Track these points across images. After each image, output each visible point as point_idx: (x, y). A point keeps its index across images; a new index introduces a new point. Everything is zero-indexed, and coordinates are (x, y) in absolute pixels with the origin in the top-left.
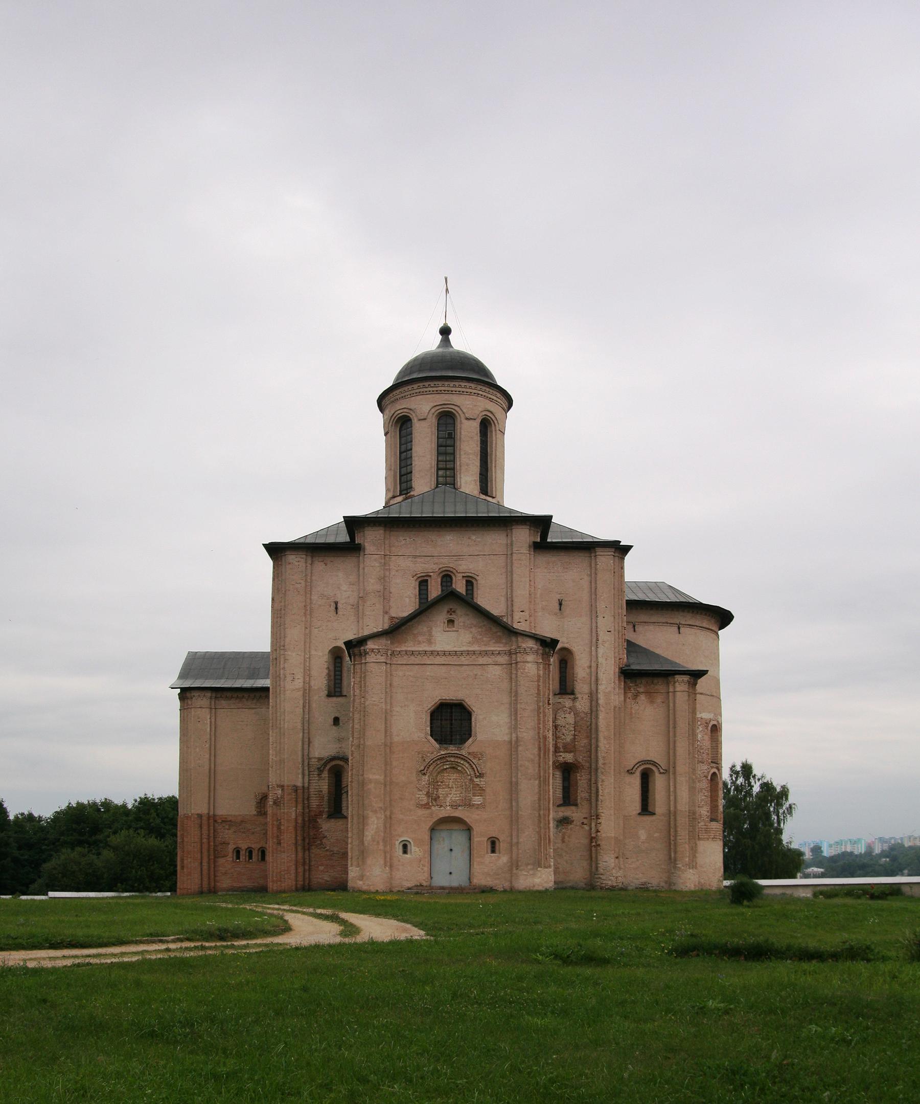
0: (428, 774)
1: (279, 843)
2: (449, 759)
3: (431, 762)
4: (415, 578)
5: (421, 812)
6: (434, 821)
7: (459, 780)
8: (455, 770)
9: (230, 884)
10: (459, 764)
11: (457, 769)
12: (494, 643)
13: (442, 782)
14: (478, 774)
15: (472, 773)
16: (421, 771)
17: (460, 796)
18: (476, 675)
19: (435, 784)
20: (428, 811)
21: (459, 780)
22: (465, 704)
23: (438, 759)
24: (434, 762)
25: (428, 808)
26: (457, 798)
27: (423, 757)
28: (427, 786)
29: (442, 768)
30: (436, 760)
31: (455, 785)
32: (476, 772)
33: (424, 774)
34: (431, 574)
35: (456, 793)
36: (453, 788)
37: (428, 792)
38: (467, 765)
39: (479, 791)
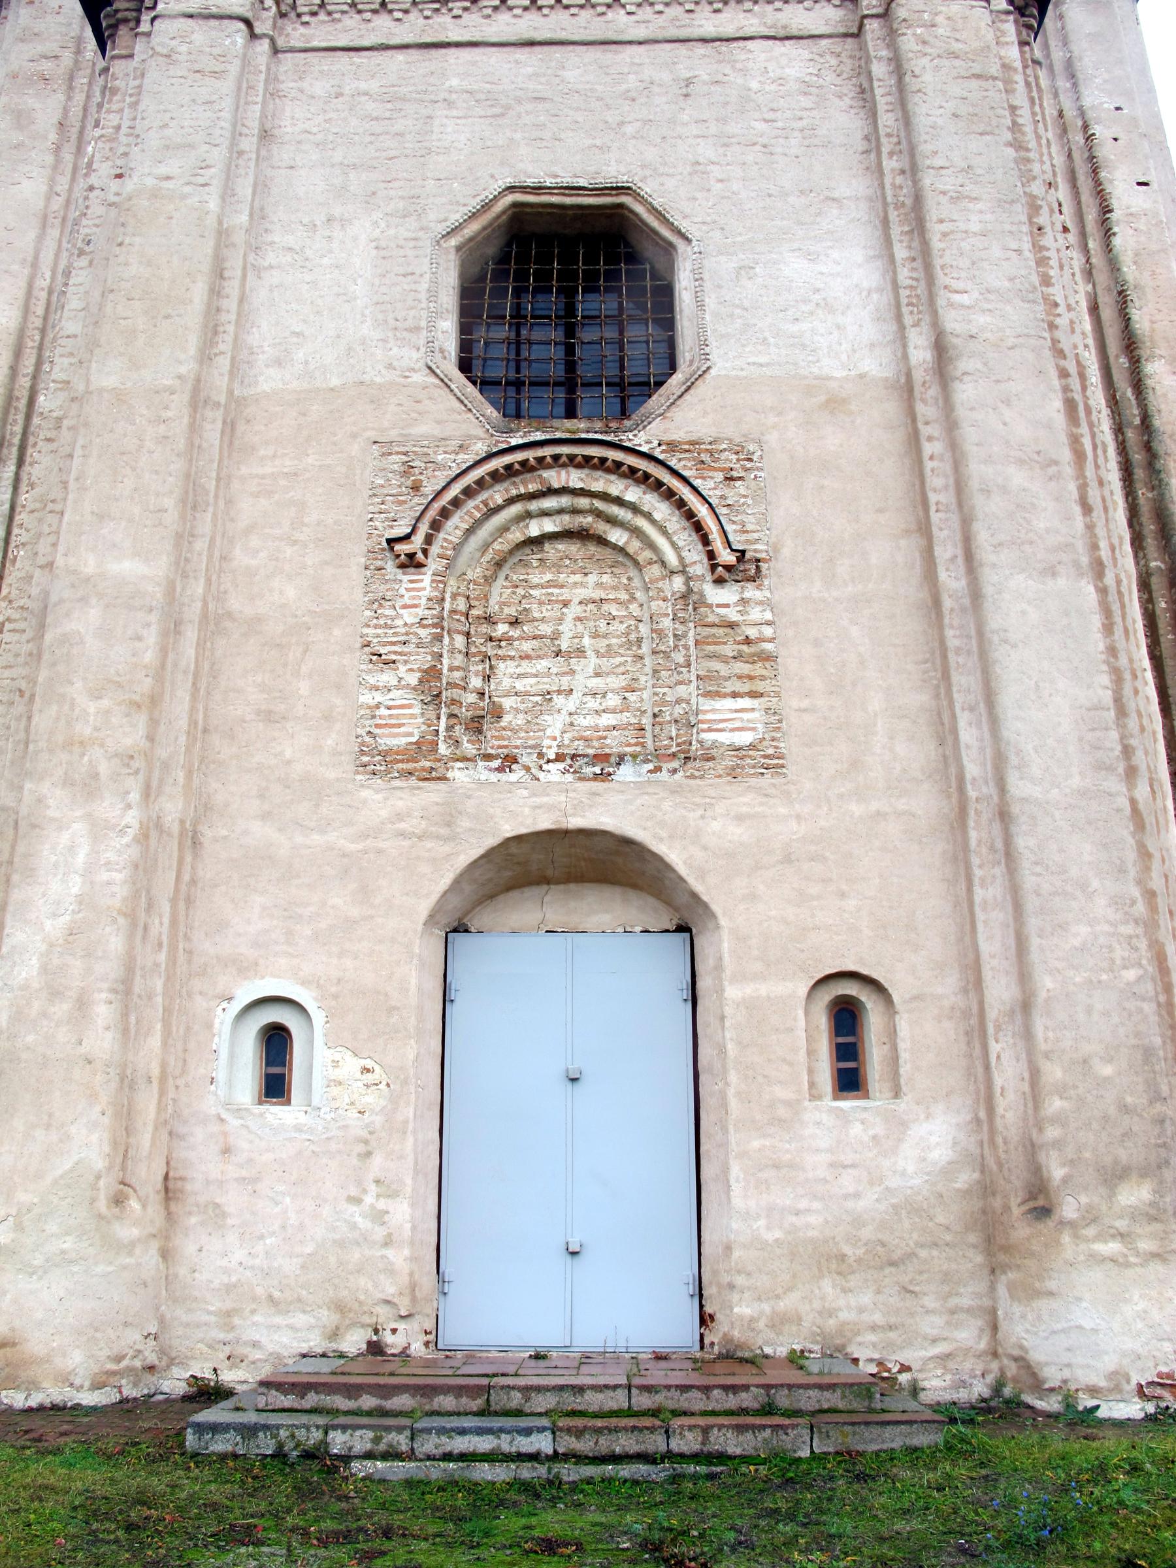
0: (434, 565)
2: (556, 478)
3: (455, 490)
6: (464, 859)
7: (614, 610)
8: (592, 548)
10: (615, 510)
11: (602, 541)
13: (515, 623)
15: (695, 556)
17: (625, 707)
18: (688, 82)
20: (433, 793)
21: (614, 610)
22: (639, 209)
23: (495, 476)
24: (468, 492)
25: (429, 776)
26: (607, 720)
27: (407, 470)
28: (423, 633)
29: (516, 536)
30: (480, 483)
31: (595, 635)
32: (718, 544)
33: (411, 563)
35: (594, 683)
36: (580, 652)
37: (431, 673)
38: (662, 510)
39: (741, 667)
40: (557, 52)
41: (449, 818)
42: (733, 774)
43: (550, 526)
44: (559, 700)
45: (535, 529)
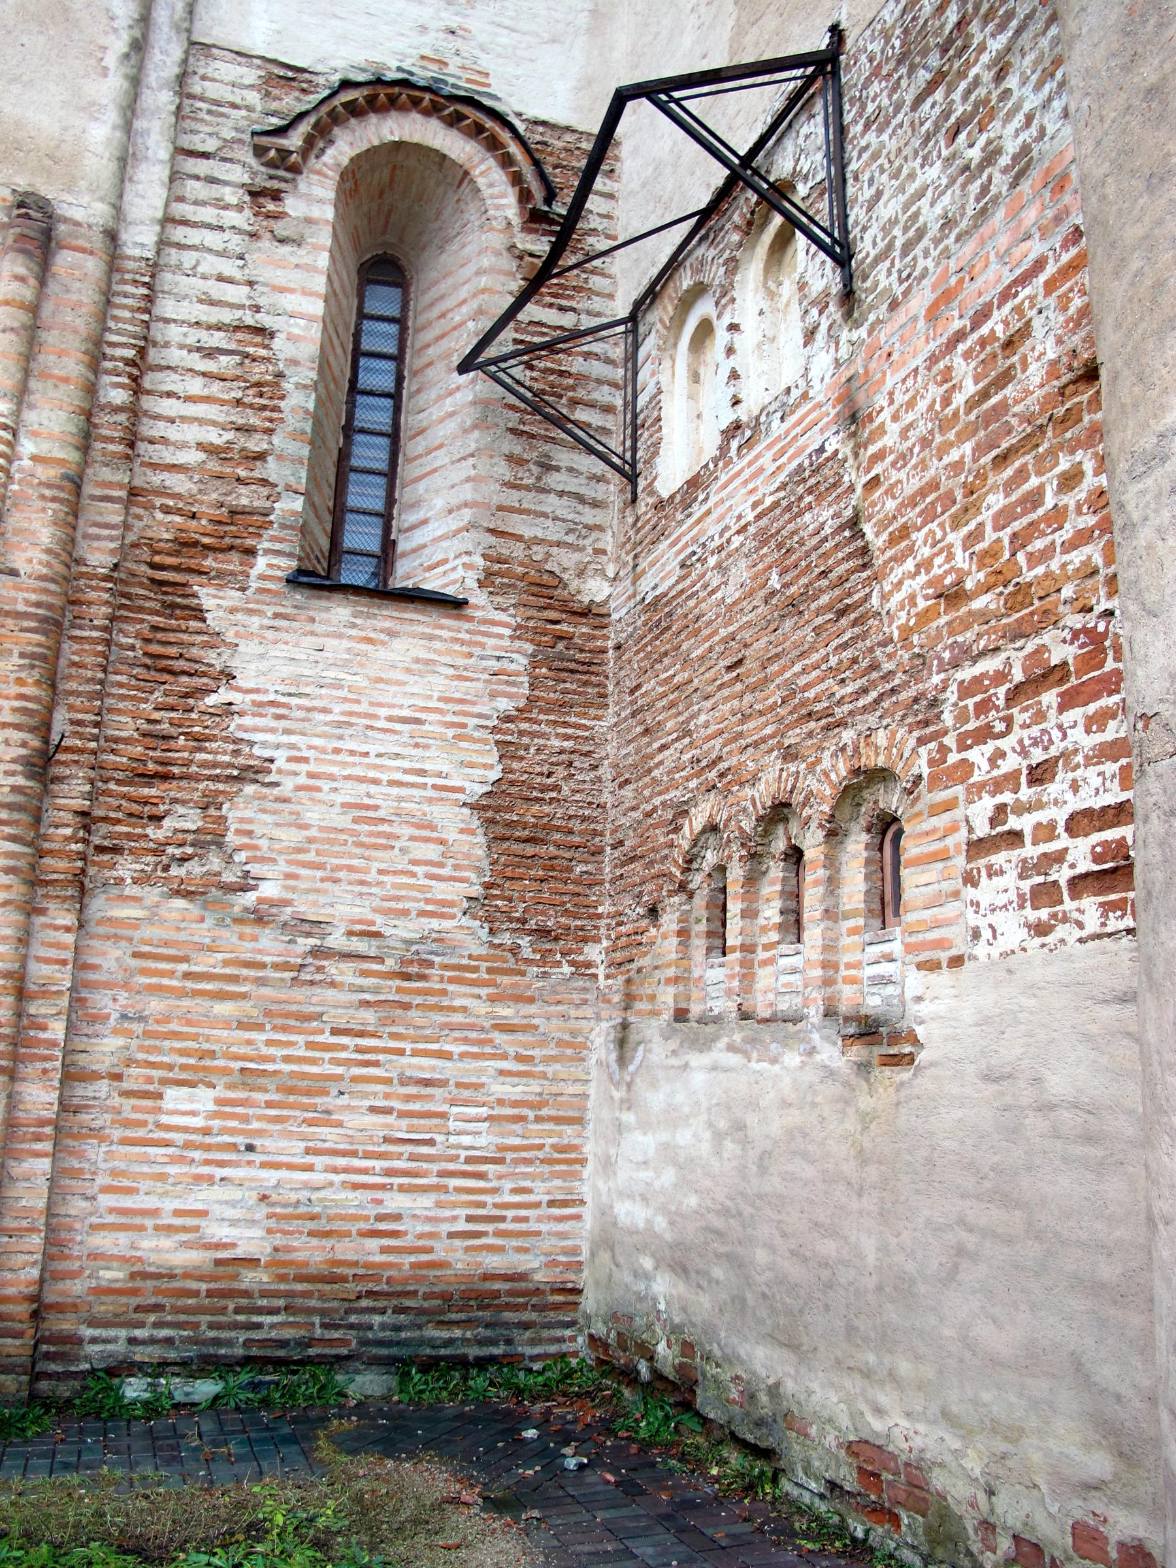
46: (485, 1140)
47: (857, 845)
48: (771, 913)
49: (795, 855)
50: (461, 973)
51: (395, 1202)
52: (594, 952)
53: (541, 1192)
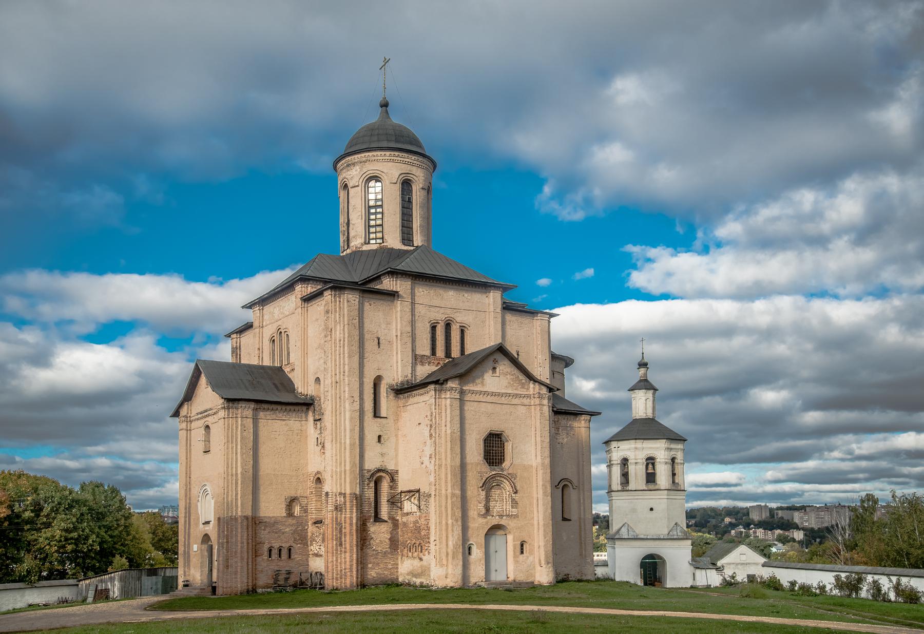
1: (341, 545)
4: (430, 323)
5: (482, 521)
9: (265, 581)
12: (521, 388)
14: (515, 491)
16: (481, 487)
19: (488, 498)
20: (485, 520)
27: (481, 476)
34: (440, 322)
36: (497, 501)
38: (508, 483)
39: (515, 505)
40: (496, 405)
41: (487, 523)
42: (514, 518)
43: (495, 484)
44: (495, 507)
45: (493, 485)
46: (391, 567)
47: (420, 547)
48: (414, 550)
49: (416, 546)
50: (389, 553)
51: (385, 572)
52: (399, 551)
53: (395, 571)
